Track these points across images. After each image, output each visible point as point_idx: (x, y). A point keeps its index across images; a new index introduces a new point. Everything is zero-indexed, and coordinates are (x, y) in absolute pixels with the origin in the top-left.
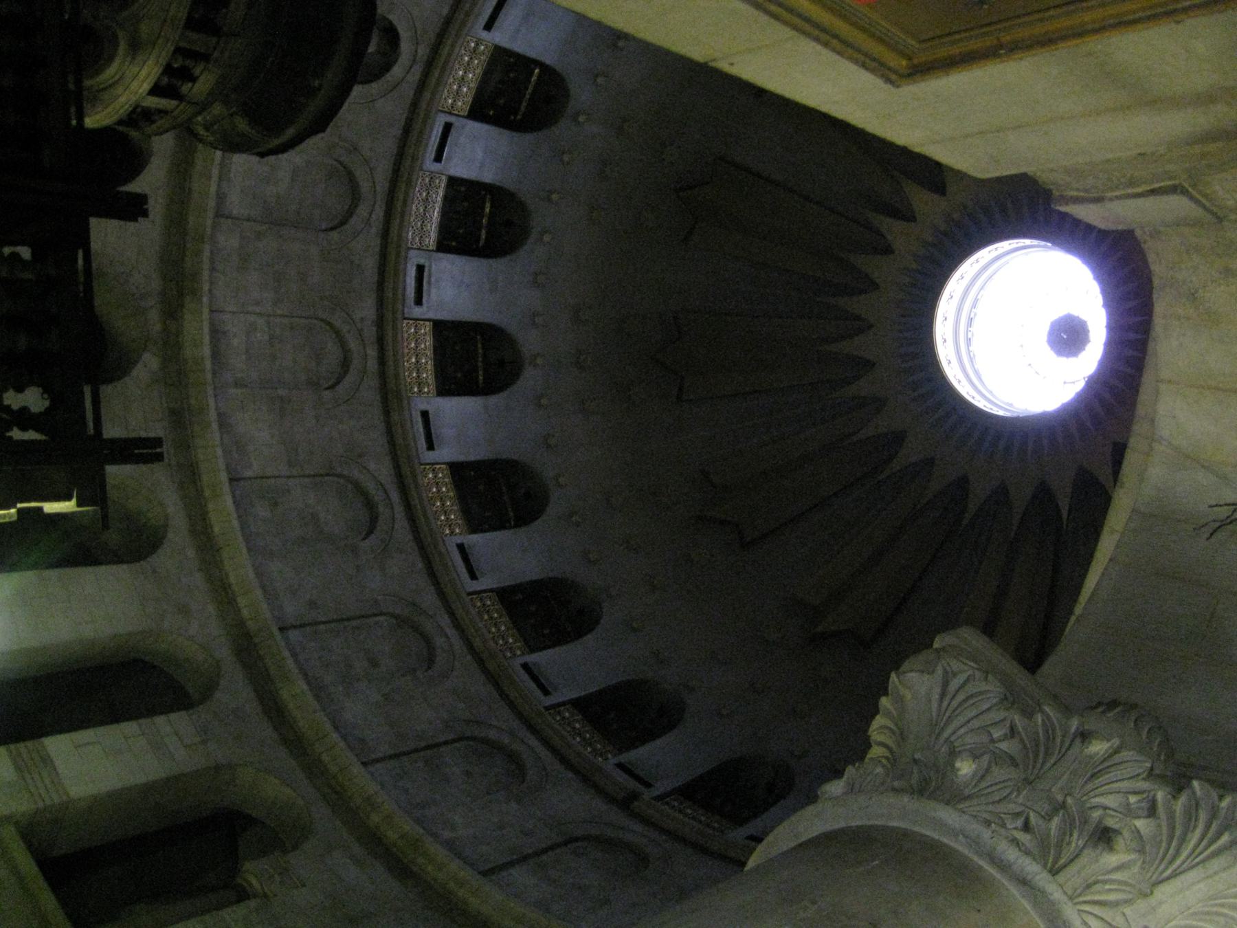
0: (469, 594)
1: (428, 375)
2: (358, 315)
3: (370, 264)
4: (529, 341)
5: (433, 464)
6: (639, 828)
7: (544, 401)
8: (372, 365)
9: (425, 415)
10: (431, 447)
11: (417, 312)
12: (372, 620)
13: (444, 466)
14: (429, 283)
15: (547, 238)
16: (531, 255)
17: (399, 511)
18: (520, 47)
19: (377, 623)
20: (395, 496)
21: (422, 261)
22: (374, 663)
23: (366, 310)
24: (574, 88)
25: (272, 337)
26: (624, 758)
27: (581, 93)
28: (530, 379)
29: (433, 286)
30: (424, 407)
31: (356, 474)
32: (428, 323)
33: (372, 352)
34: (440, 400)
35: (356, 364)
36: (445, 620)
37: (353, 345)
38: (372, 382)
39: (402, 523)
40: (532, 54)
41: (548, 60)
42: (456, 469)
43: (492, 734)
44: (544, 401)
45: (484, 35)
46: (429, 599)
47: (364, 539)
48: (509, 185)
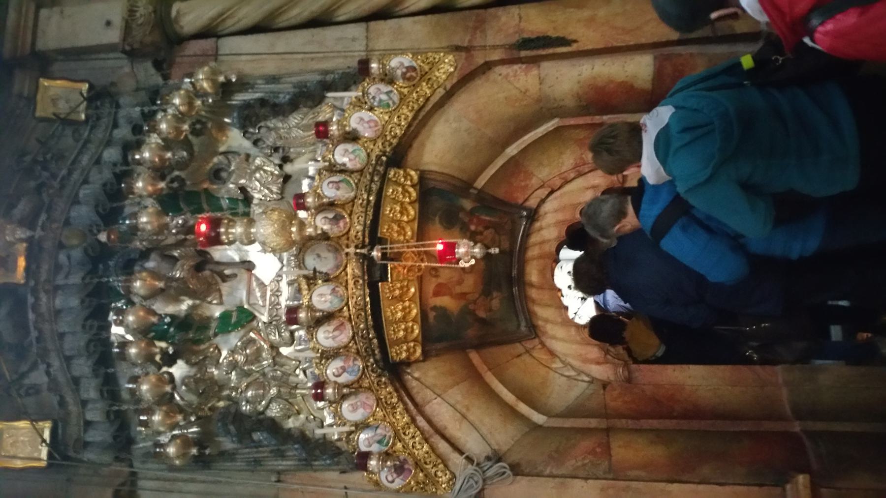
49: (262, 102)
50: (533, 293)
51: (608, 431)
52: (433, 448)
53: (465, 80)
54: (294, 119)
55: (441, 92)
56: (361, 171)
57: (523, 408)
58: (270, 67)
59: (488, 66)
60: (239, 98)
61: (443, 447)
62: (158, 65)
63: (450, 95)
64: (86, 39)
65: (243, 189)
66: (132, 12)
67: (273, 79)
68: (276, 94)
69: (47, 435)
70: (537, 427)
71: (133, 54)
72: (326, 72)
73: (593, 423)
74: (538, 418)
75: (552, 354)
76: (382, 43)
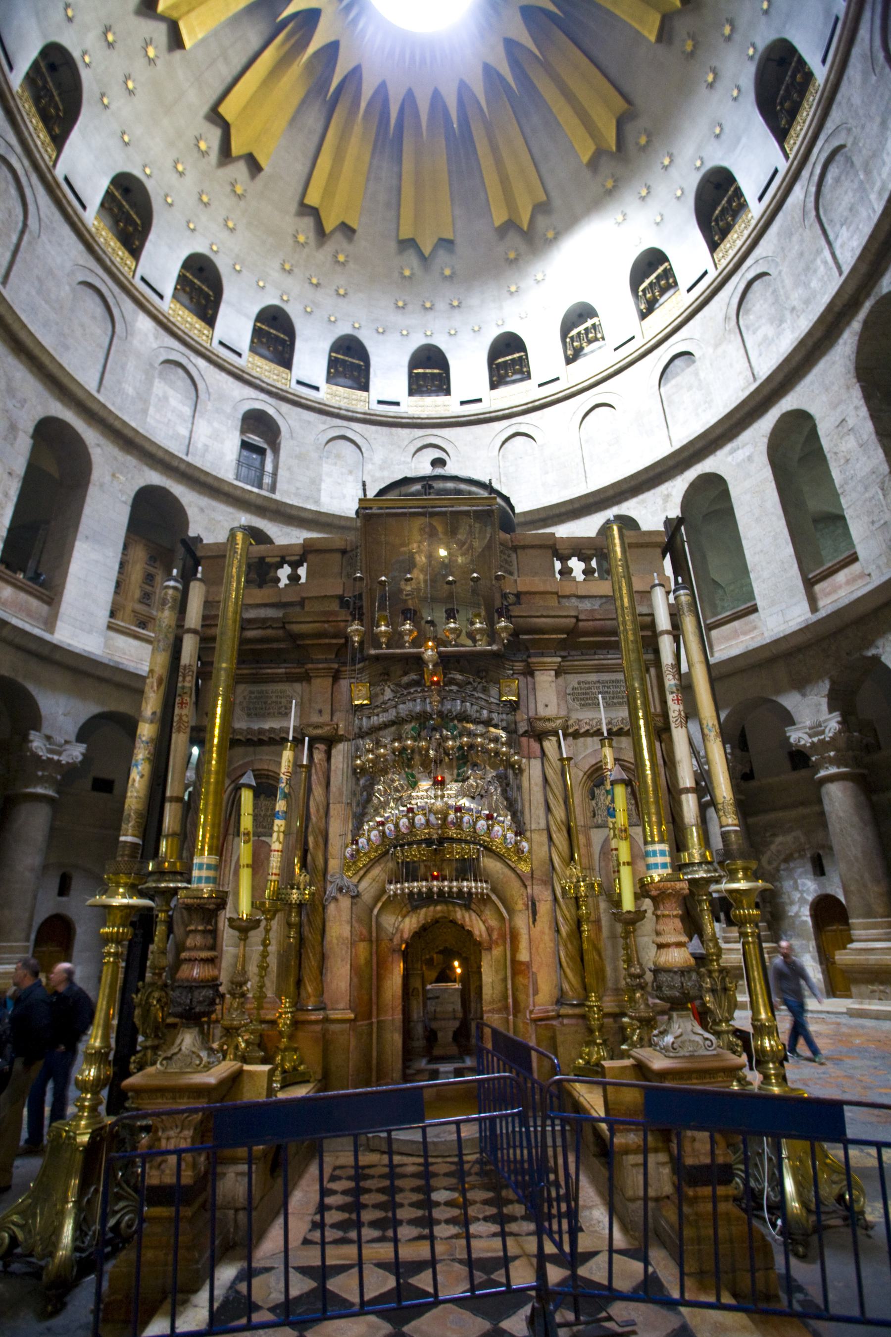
49: (508, 785)
50: (432, 908)
51: (371, 941)
52: (361, 869)
53: (519, 876)
54: (501, 799)
55: (513, 865)
56: (475, 832)
57: (379, 905)
58: (525, 784)
59: (525, 886)
60: (510, 772)
61: (362, 872)
62: (526, 732)
63: (513, 870)
64: (539, 694)
65: (468, 778)
66: (549, 720)
67: (519, 788)
68: (512, 789)
69: (365, 702)
70: (371, 911)
71: (530, 721)
72: (522, 813)
73: (374, 935)
74: (376, 911)
75: (404, 917)
76: (535, 837)
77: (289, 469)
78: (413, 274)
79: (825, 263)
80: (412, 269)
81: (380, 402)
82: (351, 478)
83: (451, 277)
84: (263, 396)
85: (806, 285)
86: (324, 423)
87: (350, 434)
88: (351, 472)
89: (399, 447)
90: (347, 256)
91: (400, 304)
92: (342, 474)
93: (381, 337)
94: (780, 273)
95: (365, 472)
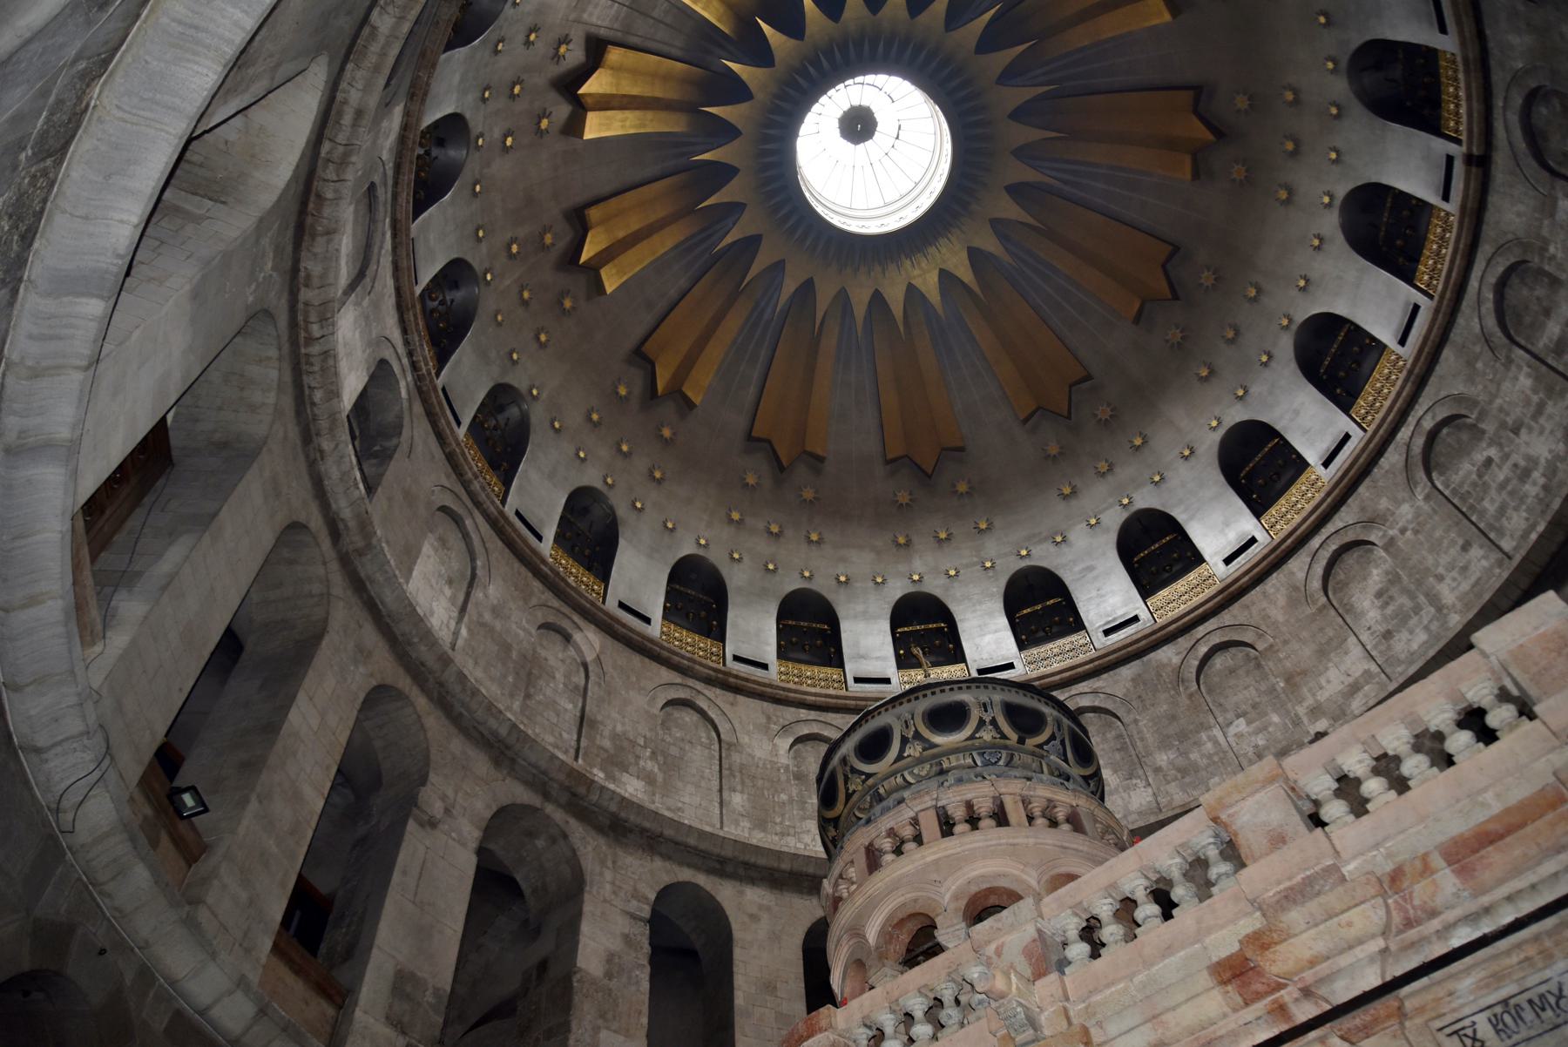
0: (1365, 430)
1: (1192, 577)
2: (1176, 660)
3: (1127, 672)
4: (1114, 519)
5: (1267, 531)
6: (1499, 126)
7: (1157, 478)
8: (1211, 624)
9: (1228, 561)
10: (1253, 541)
11: (1144, 614)
12: (1447, 493)
13: (1263, 521)
14: (1114, 620)
15: (1024, 552)
16: (1044, 556)
17: (1329, 528)
18: (889, 650)
19: (1447, 486)
20: (1316, 542)
21: (1101, 635)
22: (1489, 461)
23: (1168, 655)
24: (898, 595)
25: (1238, 717)
26: (1433, 199)
27: (897, 589)
28: (1145, 499)
29: (1115, 616)
30: (1222, 566)
31: (1316, 584)
32: (1149, 604)
33: (1201, 630)
34: (1206, 557)
35: (1216, 639)
36: (1404, 434)
37: (1203, 649)
38: (1226, 617)
39: (1337, 523)
40: (889, 639)
41: (885, 626)
42: (1258, 510)
43: (1491, 322)
44: (1157, 478)
45: (894, 680)
46: (1392, 458)
47: (1373, 544)
48: (998, 605)
77: (390, 499)
78: (626, 398)
79: (1216, 743)
80: (629, 393)
81: (518, 514)
82: (448, 592)
83: (667, 443)
84: (405, 361)
85: (1185, 754)
86: (448, 477)
87: (468, 523)
88: (450, 582)
89: (526, 600)
90: (573, 308)
91: (595, 417)
92: (440, 575)
93: (551, 433)
94: (1136, 721)
95: (472, 600)
